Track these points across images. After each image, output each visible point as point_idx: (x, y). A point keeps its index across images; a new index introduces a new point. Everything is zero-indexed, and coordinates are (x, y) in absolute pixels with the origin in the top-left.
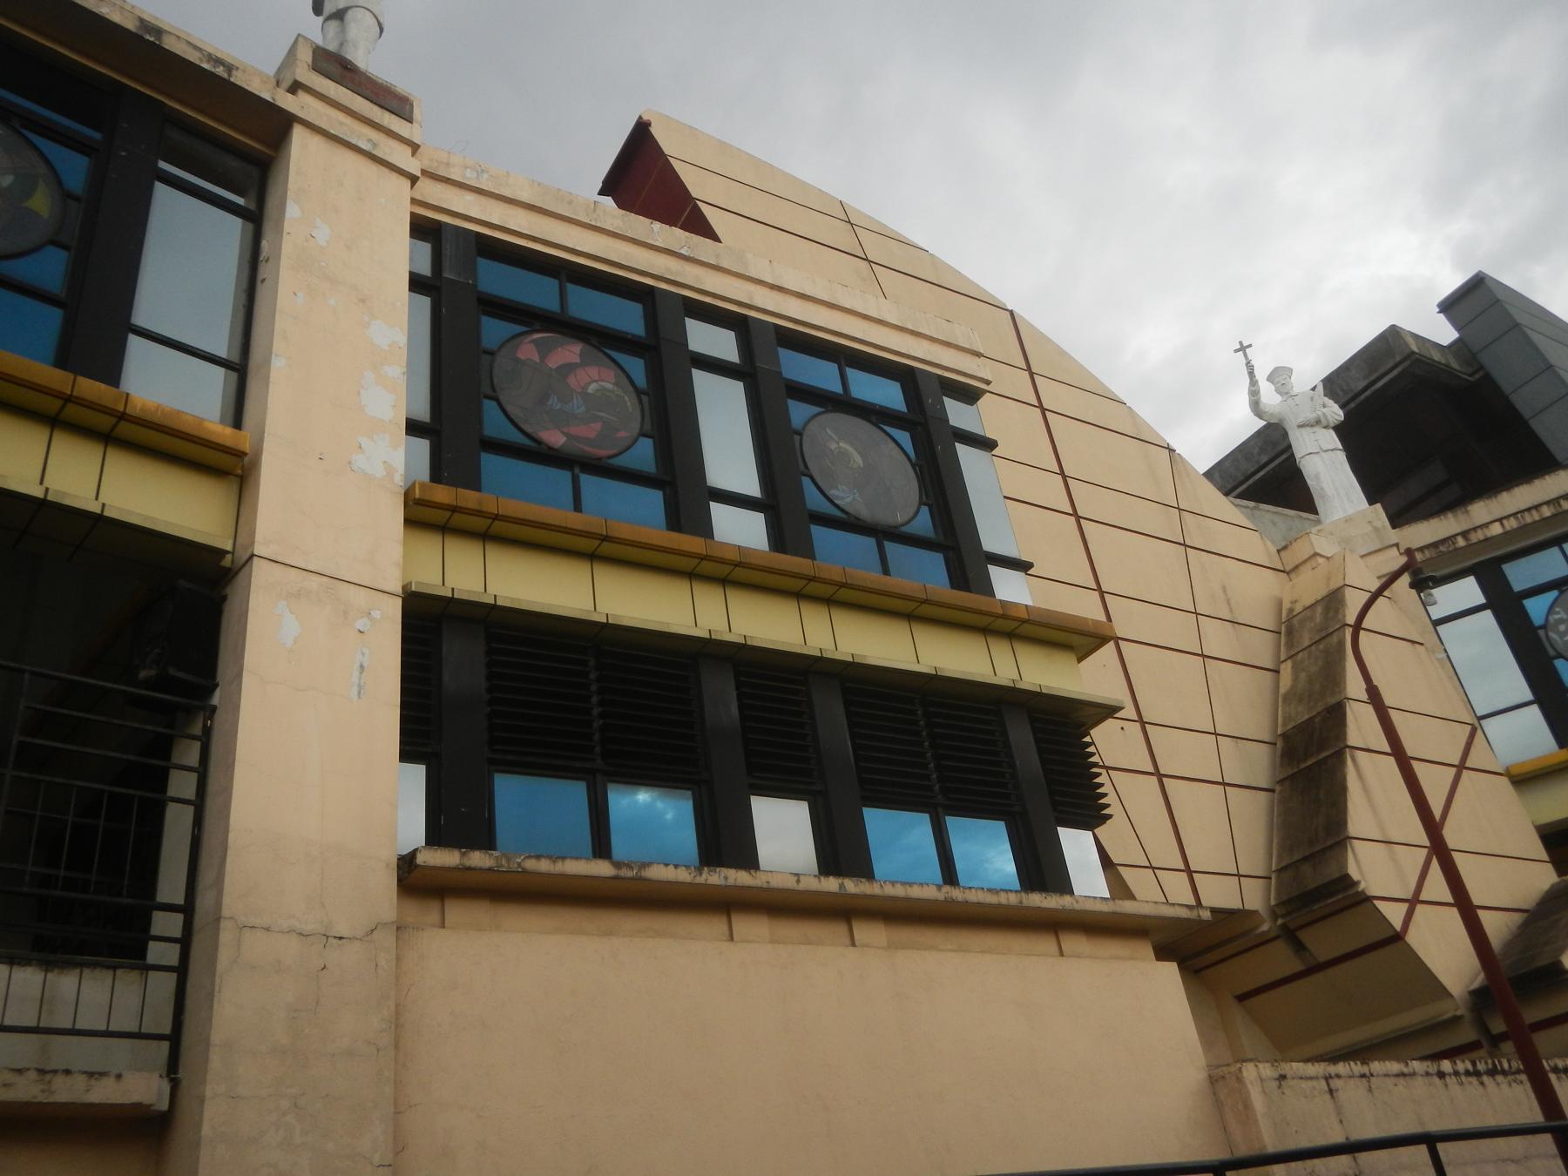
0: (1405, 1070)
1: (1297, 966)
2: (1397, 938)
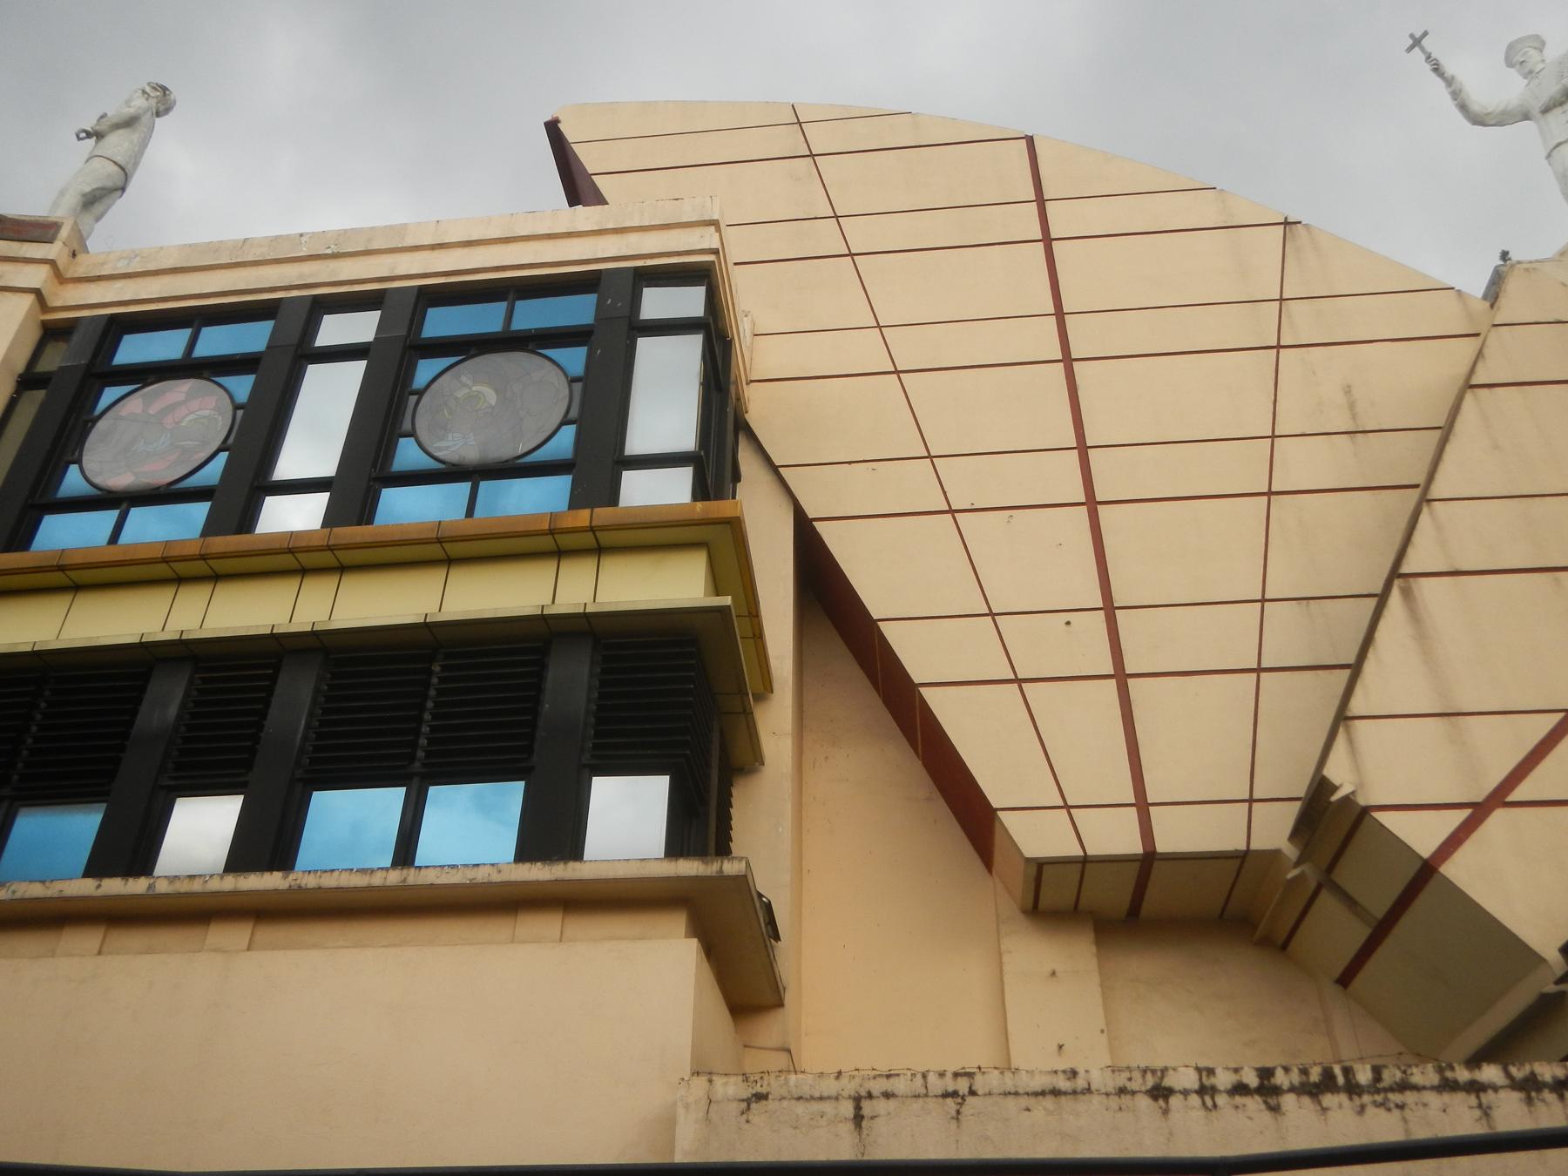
0: (1063, 1084)
1: (1359, 934)
2: (1427, 871)
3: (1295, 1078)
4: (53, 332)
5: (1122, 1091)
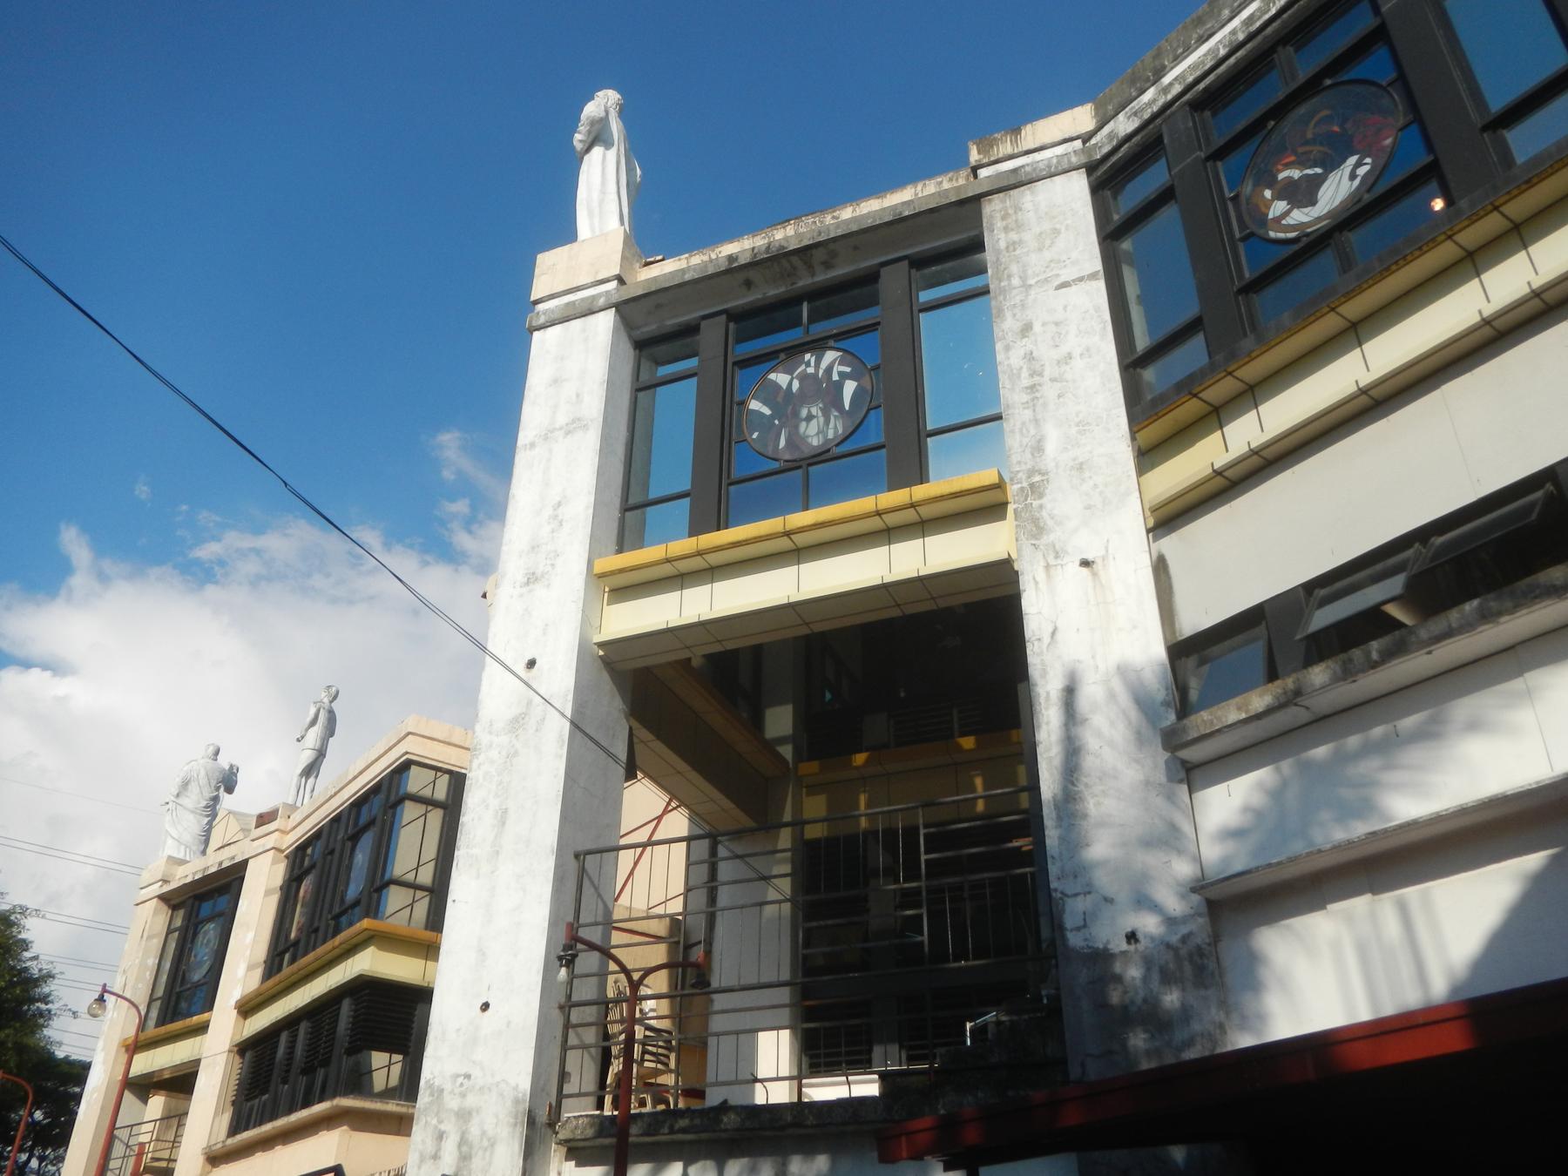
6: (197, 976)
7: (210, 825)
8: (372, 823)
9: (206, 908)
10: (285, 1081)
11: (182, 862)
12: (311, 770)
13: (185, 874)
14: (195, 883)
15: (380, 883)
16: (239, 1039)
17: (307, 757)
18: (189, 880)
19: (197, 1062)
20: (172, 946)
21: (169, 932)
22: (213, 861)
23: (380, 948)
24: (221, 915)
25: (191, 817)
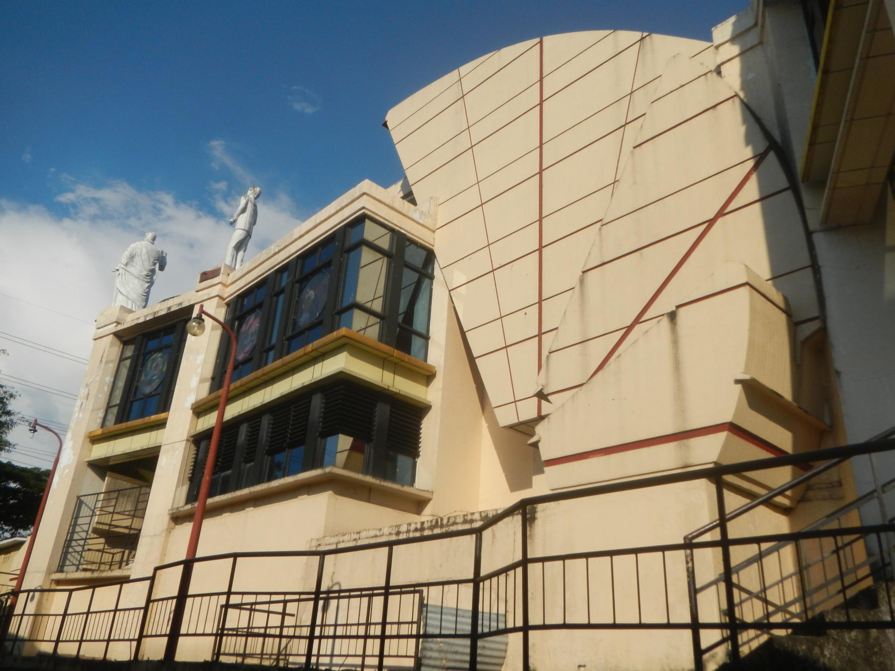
0: (378, 533)
3: (429, 524)
4: (228, 304)
5: (390, 534)
6: (147, 390)
7: (149, 287)
8: (327, 265)
9: (152, 344)
10: (247, 461)
11: (130, 311)
12: (241, 246)
13: (140, 316)
14: (146, 323)
15: (338, 309)
16: (193, 432)
17: (238, 235)
18: (141, 320)
19: (160, 447)
20: (124, 372)
21: (122, 360)
22: (159, 307)
23: (352, 354)
24: (168, 347)
25: (136, 281)
